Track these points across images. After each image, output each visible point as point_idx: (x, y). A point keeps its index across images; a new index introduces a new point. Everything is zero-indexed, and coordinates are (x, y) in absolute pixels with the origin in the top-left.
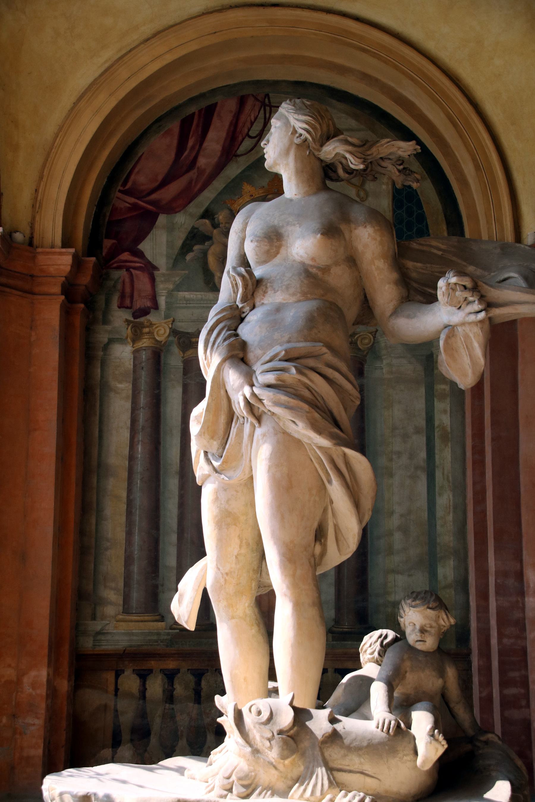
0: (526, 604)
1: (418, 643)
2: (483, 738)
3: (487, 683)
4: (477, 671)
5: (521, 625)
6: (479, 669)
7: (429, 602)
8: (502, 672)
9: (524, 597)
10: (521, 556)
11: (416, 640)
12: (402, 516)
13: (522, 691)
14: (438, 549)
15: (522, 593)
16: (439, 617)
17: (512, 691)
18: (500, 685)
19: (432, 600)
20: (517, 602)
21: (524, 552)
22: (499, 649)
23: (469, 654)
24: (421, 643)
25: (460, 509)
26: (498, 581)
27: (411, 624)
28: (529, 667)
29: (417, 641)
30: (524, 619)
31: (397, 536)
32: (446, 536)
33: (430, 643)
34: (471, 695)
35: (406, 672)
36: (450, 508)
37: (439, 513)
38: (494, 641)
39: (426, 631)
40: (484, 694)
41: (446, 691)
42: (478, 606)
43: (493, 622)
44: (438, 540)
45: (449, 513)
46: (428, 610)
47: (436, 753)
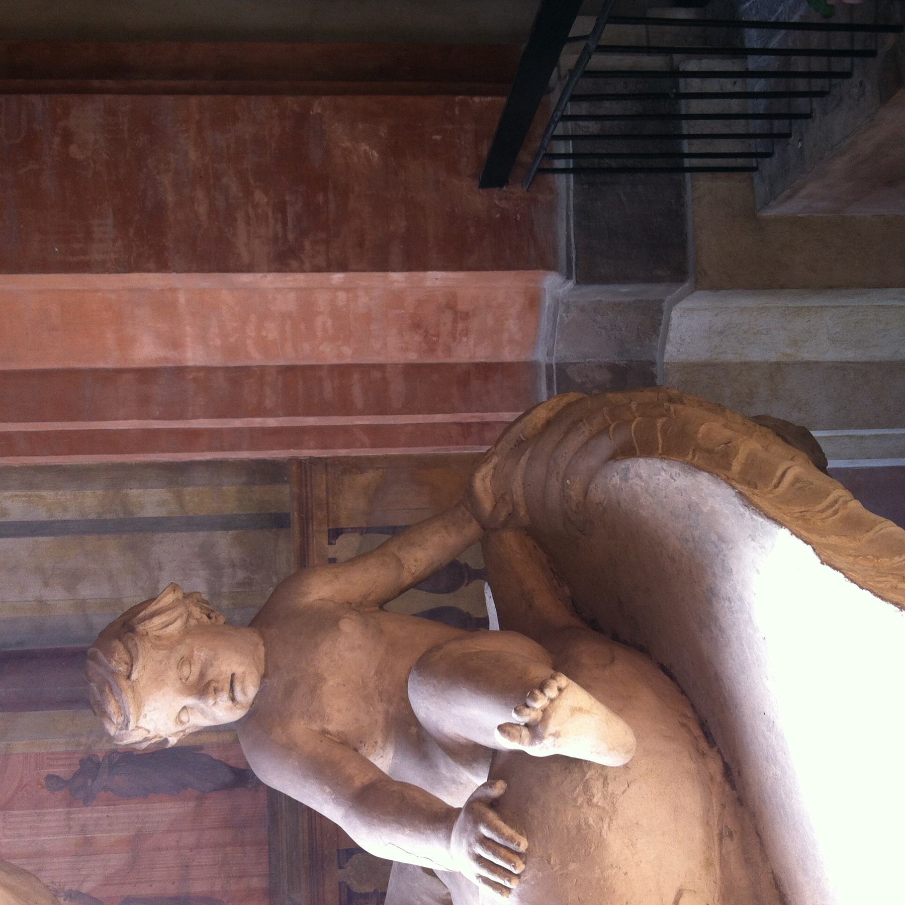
0: (199, 363)
1: (239, 695)
2: (487, 505)
3: (346, 435)
4: (325, 451)
5: (238, 375)
6: (322, 448)
7: (113, 673)
8: (324, 410)
9: (187, 367)
10: (107, 370)
11: (230, 703)
12: (46, 584)
13: (356, 376)
14: (109, 516)
15: (180, 371)
16: (158, 637)
17: (357, 391)
18: (348, 413)
19: (105, 661)
20: (195, 380)
21: (101, 365)
22: (286, 415)
23: (299, 462)
24: (238, 688)
25: (32, 478)
26: (158, 413)
27: (184, 718)
28: (313, 362)
29: (233, 699)
30: (227, 369)
31: (86, 591)
32: (87, 501)
33: (240, 666)
34: (368, 458)
35: (324, 732)
36: (30, 496)
37: (41, 515)
38: (272, 422)
39: (202, 675)
40: (365, 439)
41: (371, 598)
42: (211, 449)
43: (237, 423)
44: (93, 516)
45: (40, 497)
46: (134, 676)
47: (588, 712)
